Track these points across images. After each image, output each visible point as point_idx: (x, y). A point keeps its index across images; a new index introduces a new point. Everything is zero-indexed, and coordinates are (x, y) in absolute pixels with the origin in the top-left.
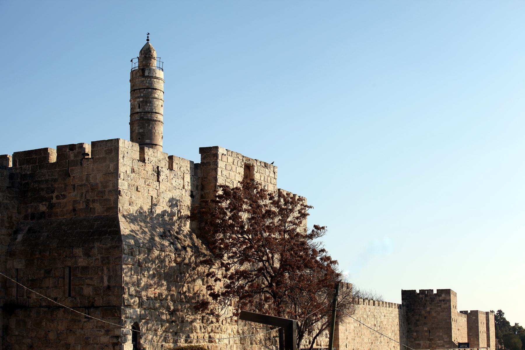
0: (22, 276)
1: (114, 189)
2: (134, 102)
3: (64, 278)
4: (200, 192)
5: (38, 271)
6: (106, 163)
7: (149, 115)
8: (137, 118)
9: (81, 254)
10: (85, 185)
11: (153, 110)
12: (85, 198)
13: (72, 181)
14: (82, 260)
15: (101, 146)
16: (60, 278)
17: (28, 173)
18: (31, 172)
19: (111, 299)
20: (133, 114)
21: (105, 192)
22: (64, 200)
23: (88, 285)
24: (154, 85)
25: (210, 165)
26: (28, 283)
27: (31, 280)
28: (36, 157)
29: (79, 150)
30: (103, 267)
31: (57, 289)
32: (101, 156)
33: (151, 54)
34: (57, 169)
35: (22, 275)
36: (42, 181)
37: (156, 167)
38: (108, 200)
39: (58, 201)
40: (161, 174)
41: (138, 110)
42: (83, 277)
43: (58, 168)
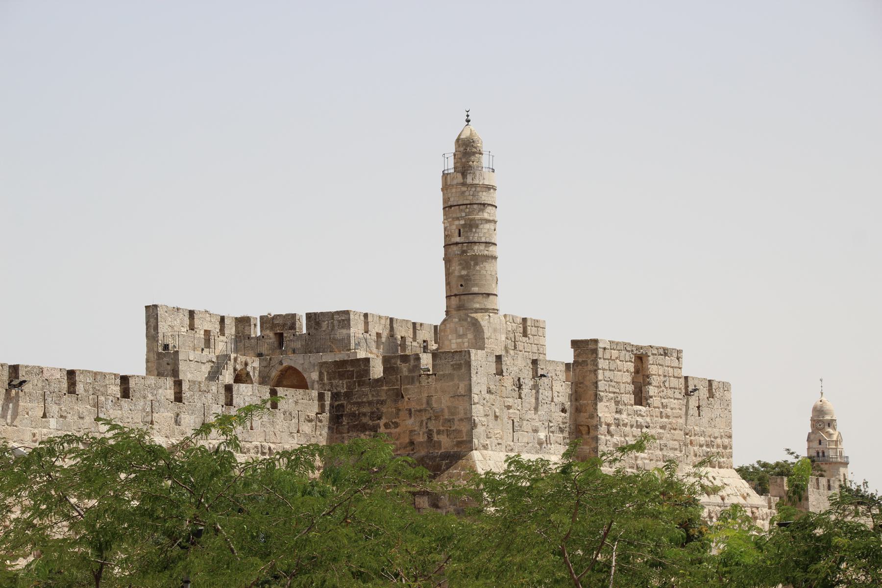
2: (450, 225)
4: (574, 403)
7: (476, 248)
8: (456, 253)
9: (426, 505)
10: (425, 410)
11: (482, 238)
12: (427, 428)
13: (407, 405)
15: (446, 359)
17: (342, 391)
18: (345, 390)
20: (450, 245)
21: (454, 420)
24: (481, 197)
25: (587, 365)
32: (447, 372)
36: (363, 402)
37: (517, 379)
38: (460, 432)
39: (388, 431)
40: (523, 387)
41: (458, 239)
43: (387, 387)
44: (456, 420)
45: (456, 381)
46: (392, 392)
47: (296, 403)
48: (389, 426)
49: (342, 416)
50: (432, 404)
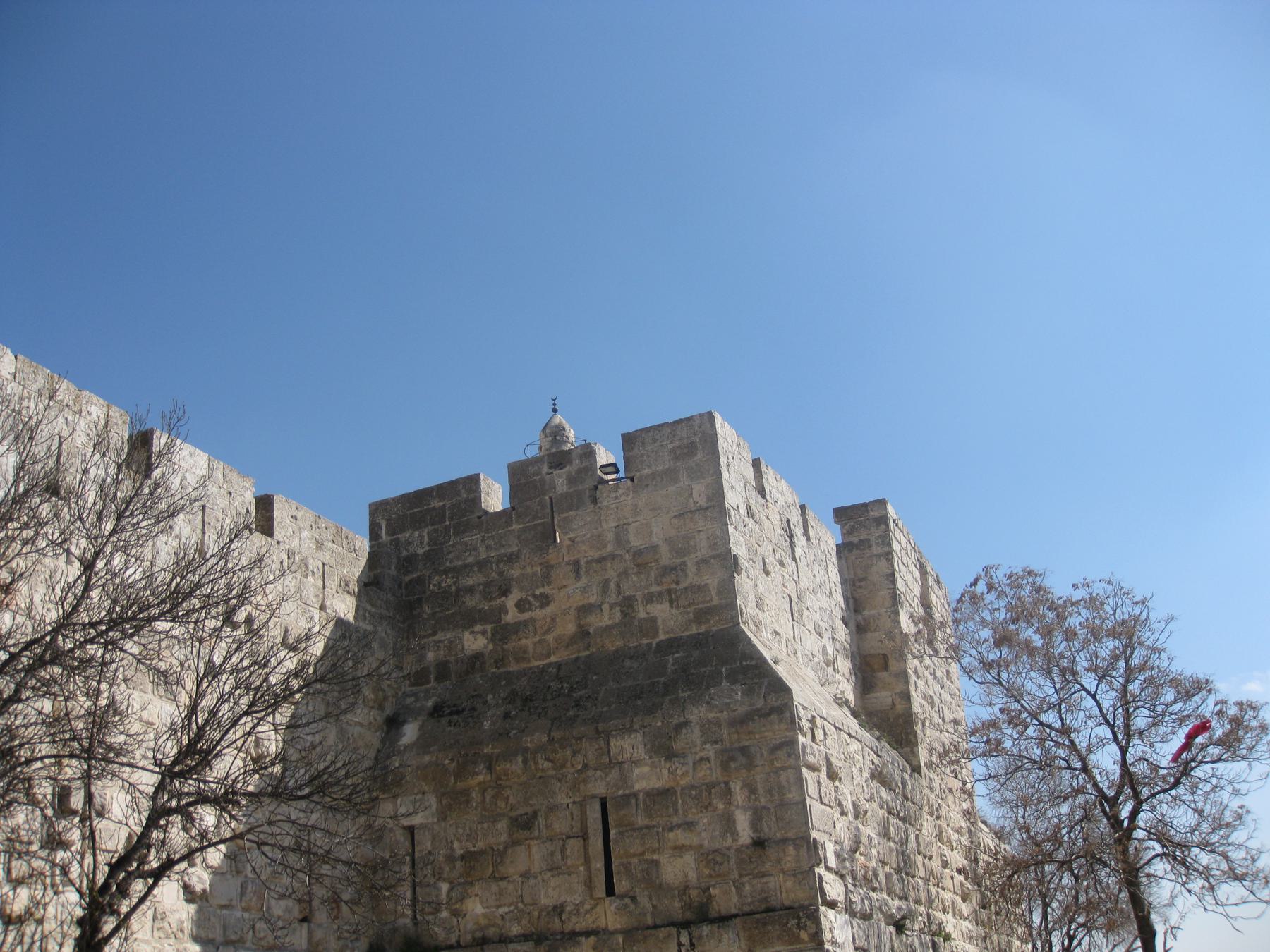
0: (429, 848)
1: (714, 553)
3: (584, 837)
5: (485, 825)
6: (677, 485)
9: (641, 752)
10: (613, 557)
13: (568, 553)
14: (646, 769)
15: (655, 440)
16: (569, 837)
17: (420, 551)
18: (427, 548)
19: (771, 885)
21: (685, 566)
22: (544, 611)
23: (679, 849)
25: (870, 546)
26: (454, 867)
27: (463, 857)
28: (442, 504)
29: (582, 463)
30: (726, 783)
31: (559, 874)
32: (660, 468)
33: (566, 434)
34: (514, 527)
35: (428, 845)
36: (466, 566)
38: (702, 588)
39: (526, 616)
42: (654, 826)
43: (518, 523)
44: (689, 564)
45: (684, 482)
46: (533, 532)
47: (320, 545)
48: (527, 606)
49: (419, 601)
50: (628, 541)
